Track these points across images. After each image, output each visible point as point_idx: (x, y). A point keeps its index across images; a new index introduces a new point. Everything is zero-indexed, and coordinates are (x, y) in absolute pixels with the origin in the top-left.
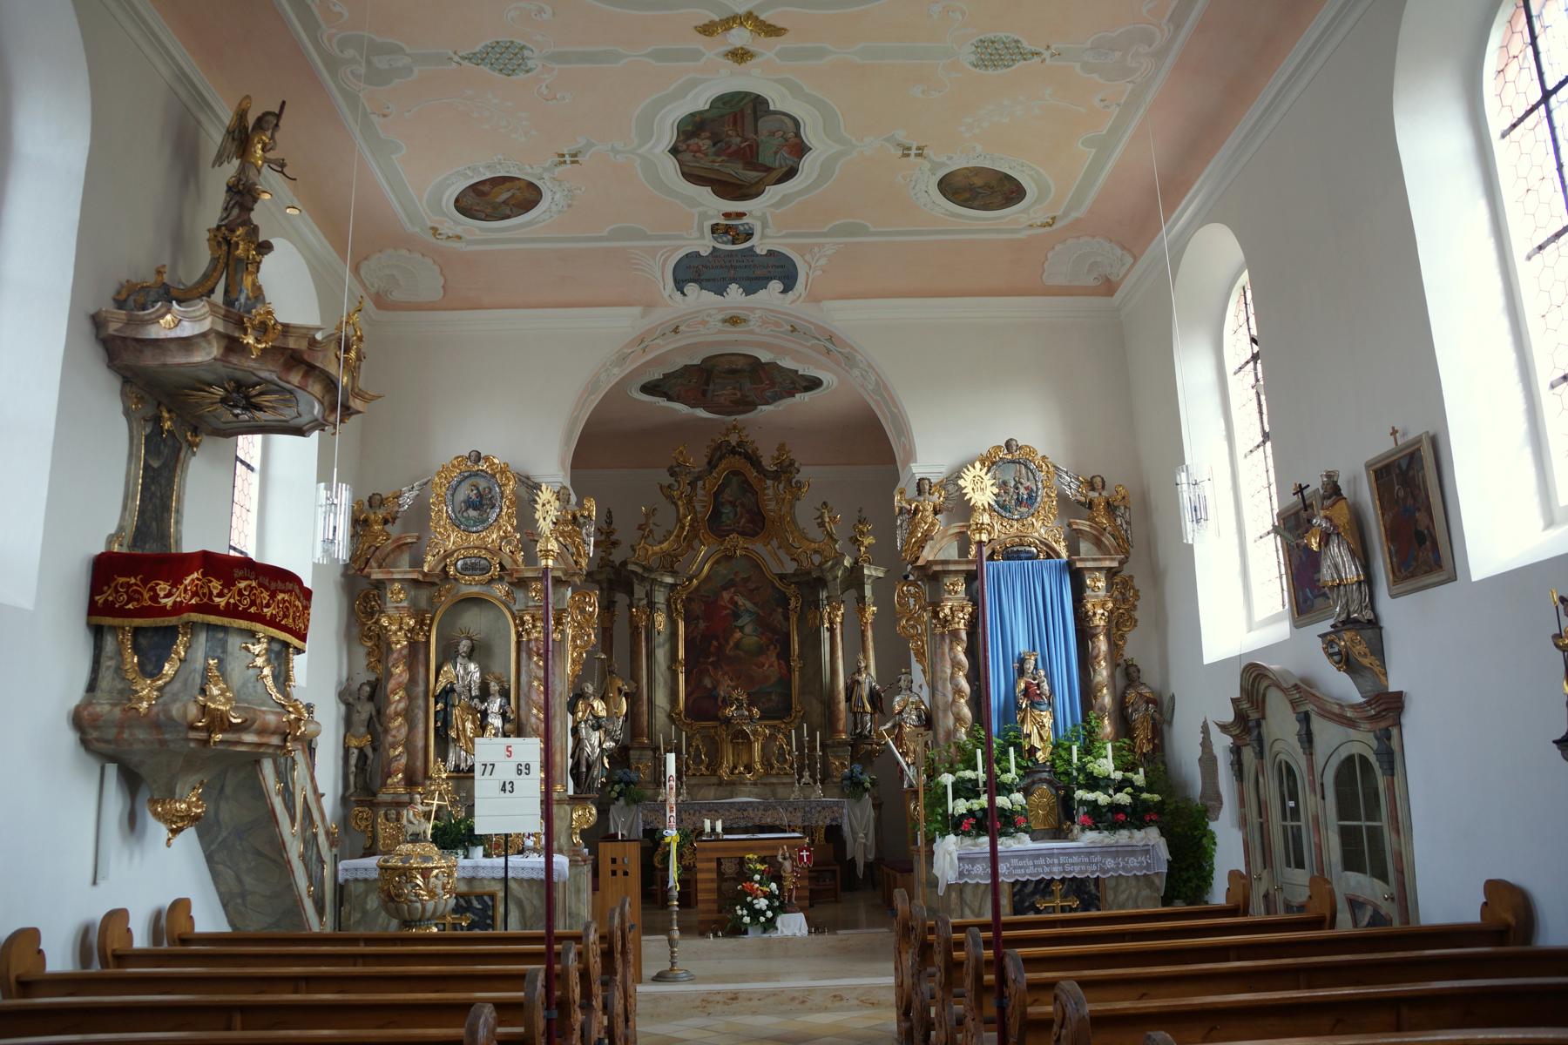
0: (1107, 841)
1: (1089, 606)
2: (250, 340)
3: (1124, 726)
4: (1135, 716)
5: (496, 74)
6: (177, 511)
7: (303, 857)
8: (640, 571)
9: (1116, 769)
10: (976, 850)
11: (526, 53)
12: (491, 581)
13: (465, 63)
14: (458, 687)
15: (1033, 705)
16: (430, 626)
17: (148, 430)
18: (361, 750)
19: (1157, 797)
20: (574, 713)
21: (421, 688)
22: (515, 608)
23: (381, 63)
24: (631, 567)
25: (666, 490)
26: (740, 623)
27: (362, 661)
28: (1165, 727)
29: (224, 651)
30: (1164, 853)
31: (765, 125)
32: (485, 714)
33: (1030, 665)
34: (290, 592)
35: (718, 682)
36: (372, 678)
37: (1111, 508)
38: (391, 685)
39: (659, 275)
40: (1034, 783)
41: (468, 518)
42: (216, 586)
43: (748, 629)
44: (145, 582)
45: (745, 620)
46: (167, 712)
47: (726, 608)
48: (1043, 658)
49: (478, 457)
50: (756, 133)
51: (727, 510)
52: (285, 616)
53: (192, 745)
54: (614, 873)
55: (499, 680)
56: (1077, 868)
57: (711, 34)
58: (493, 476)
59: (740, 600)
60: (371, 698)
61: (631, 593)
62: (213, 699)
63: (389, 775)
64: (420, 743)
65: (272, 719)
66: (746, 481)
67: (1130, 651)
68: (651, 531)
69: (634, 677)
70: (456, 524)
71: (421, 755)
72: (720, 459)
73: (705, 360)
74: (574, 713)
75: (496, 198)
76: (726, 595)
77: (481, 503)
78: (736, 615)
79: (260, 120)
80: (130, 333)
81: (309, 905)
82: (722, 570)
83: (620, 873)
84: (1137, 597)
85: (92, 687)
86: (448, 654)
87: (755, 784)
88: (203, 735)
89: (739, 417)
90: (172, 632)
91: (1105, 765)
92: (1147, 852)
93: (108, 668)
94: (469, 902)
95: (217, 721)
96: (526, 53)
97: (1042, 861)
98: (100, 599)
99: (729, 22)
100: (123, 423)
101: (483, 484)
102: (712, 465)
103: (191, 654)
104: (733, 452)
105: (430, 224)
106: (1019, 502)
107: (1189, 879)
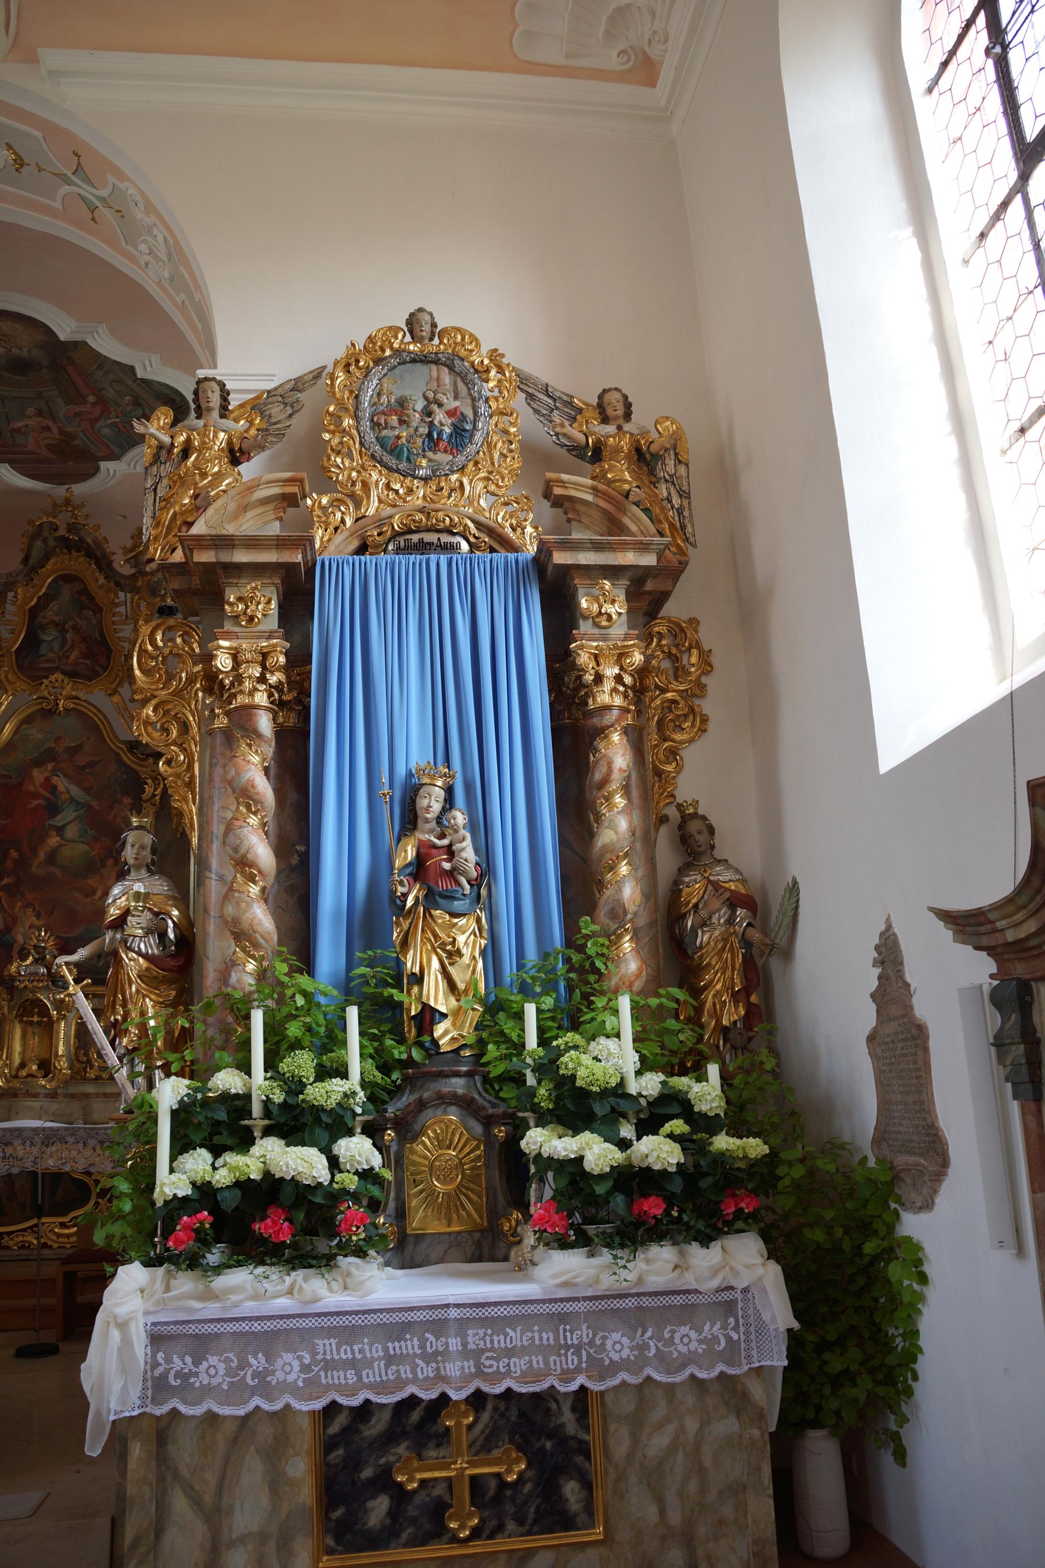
0: (607, 1283)
1: (584, 659)
3: (676, 954)
4: (703, 938)
9: (645, 1066)
10: (212, 1310)
15: (431, 899)
19: (755, 1147)
26: (59, 821)
28: (775, 964)
30: (778, 1313)
33: (432, 801)
35: (15, 920)
37: (644, 458)
40: (422, 1105)
43: (71, 832)
45: (67, 815)
47: (36, 796)
48: (468, 786)
51: (49, 636)
56: (519, 1365)
59: (61, 783)
66: (85, 591)
67: (694, 782)
72: (47, 557)
76: (38, 775)
78: (53, 809)
82: (36, 733)
84: (707, 664)
87: (53, 1095)
89: (80, 489)
91: (612, 1057)
92: (729, 1307)
97: (411, 1345)
102: (31, 568)
104: (67, 545)
106: (432, 441)
107: (848, 1377)
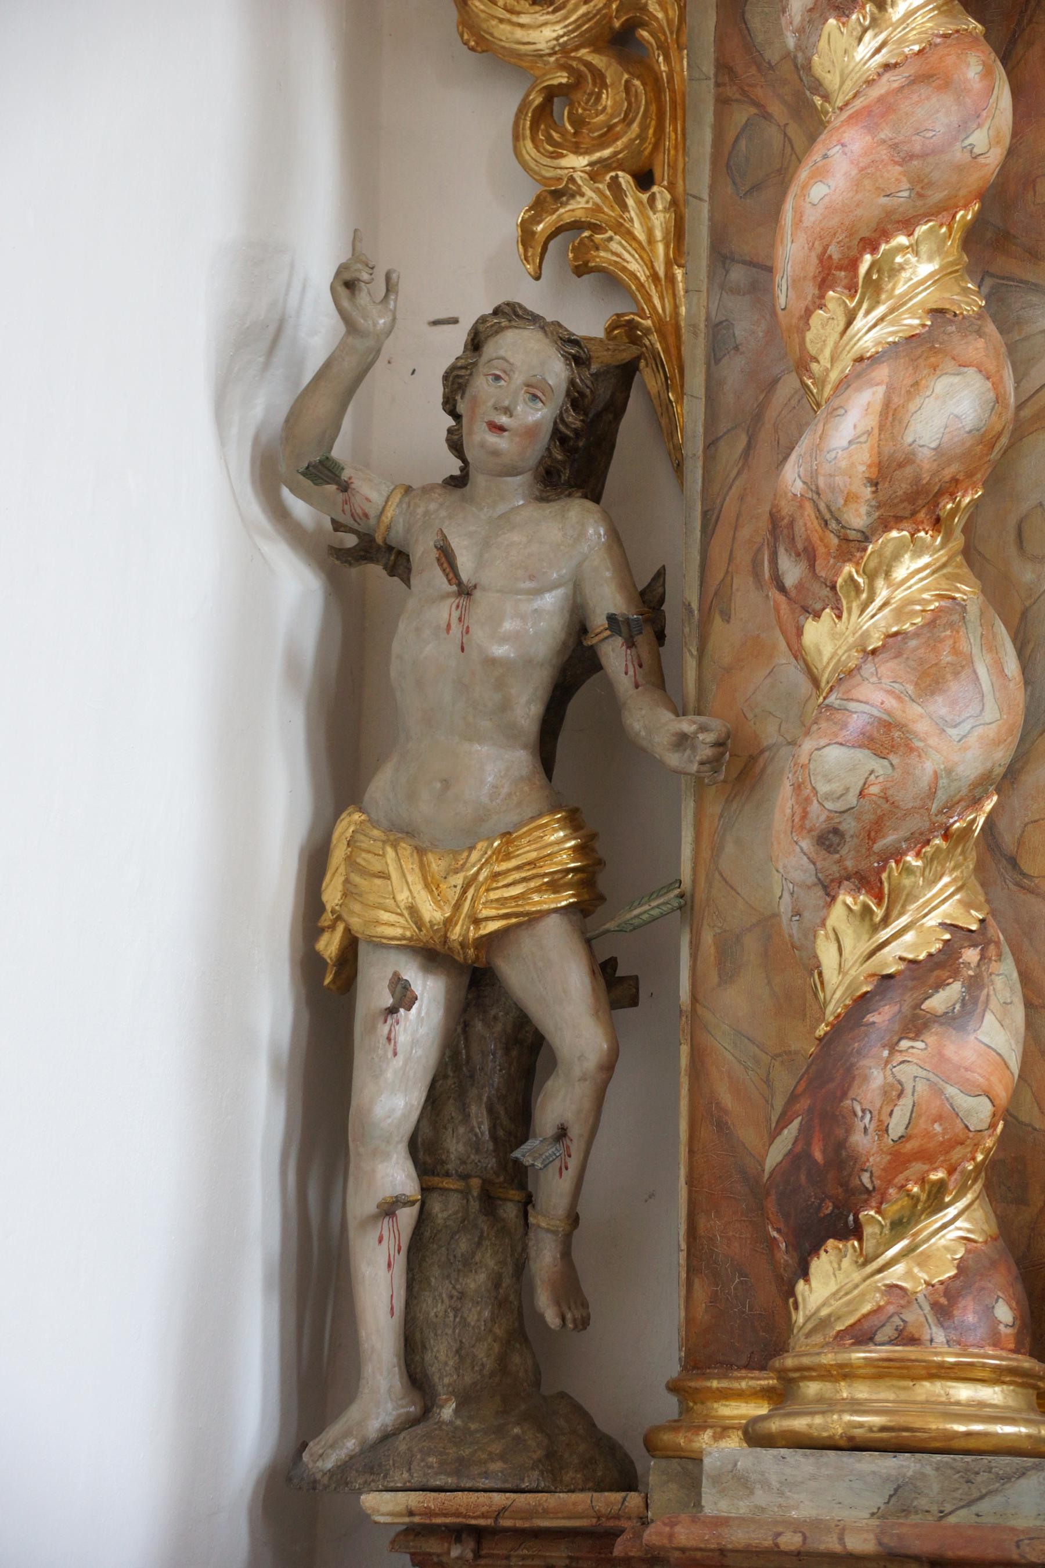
18: (476, 978)
38: (830, 183)
60: (577, 461)
63: (827, 1206)
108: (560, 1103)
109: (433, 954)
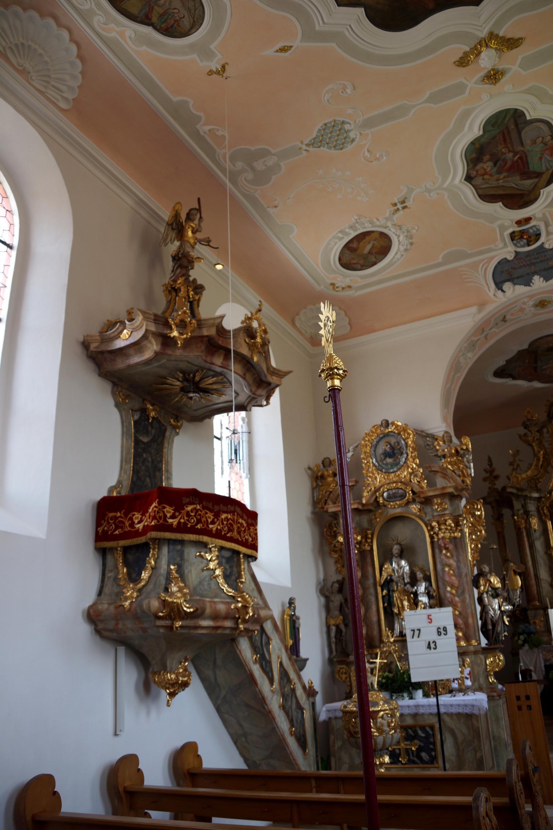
2: (175, 334)
5: (333, 151)
6: (167, 471)
7: (283, 707)
8: (514, 491)
11: (347, 127)
12: (408, 503)
13: (311, 149)
14: (394, 578)
16: (372, 539)
17: (136, 417)
18: (337, 627)
20: (478, 587)
21: (371, 581)
22: (426, 519)
23: (259, 165)
24: (509, 490)
25: (523, 438)
27: (332, 568)
29: (182, 559)
31: (527, 134)
32: (416, 594)
34: (233, 512)
36: (340, 578)
39: (483, 283)
41: (387, 464)
42: (169, 510)
44: (126, 515)
46: (141, 606)
49: (387, 424)
50: (522, 144)
52: (230, 530)
53: (162, 630)
54: (520, 708)
55: (423, 571)
57: (468, 64)
58: (399, 434)
60: (340, 590)
61: (511, 507)
62: (172, 595)
64: (375, 619)
65: (222, 608)
68: (518, 465)
69: (523, 561)
70: (379, 469)
71: (376, 627)
73: (531, 344)
74: (478, 587)
75: (364, 250)
77: (394, 453)
79: (188, 214)
80: (103, 348)
81: (292, 742)
83: (524, 708)
85: (100, 593)
86: (386, 556)
88: (168, 623)
90: (144, 548)
93: (109, 577)
94: (415, 732)
95: (174, 612)
96: (347, 127)
98: (100, 529)
99: (476, 51)
100: (115, 415)
101: (393, 441)
103: (160, 561)
105: (329, 282)
108: (343, 634)
109: (334, 625)
